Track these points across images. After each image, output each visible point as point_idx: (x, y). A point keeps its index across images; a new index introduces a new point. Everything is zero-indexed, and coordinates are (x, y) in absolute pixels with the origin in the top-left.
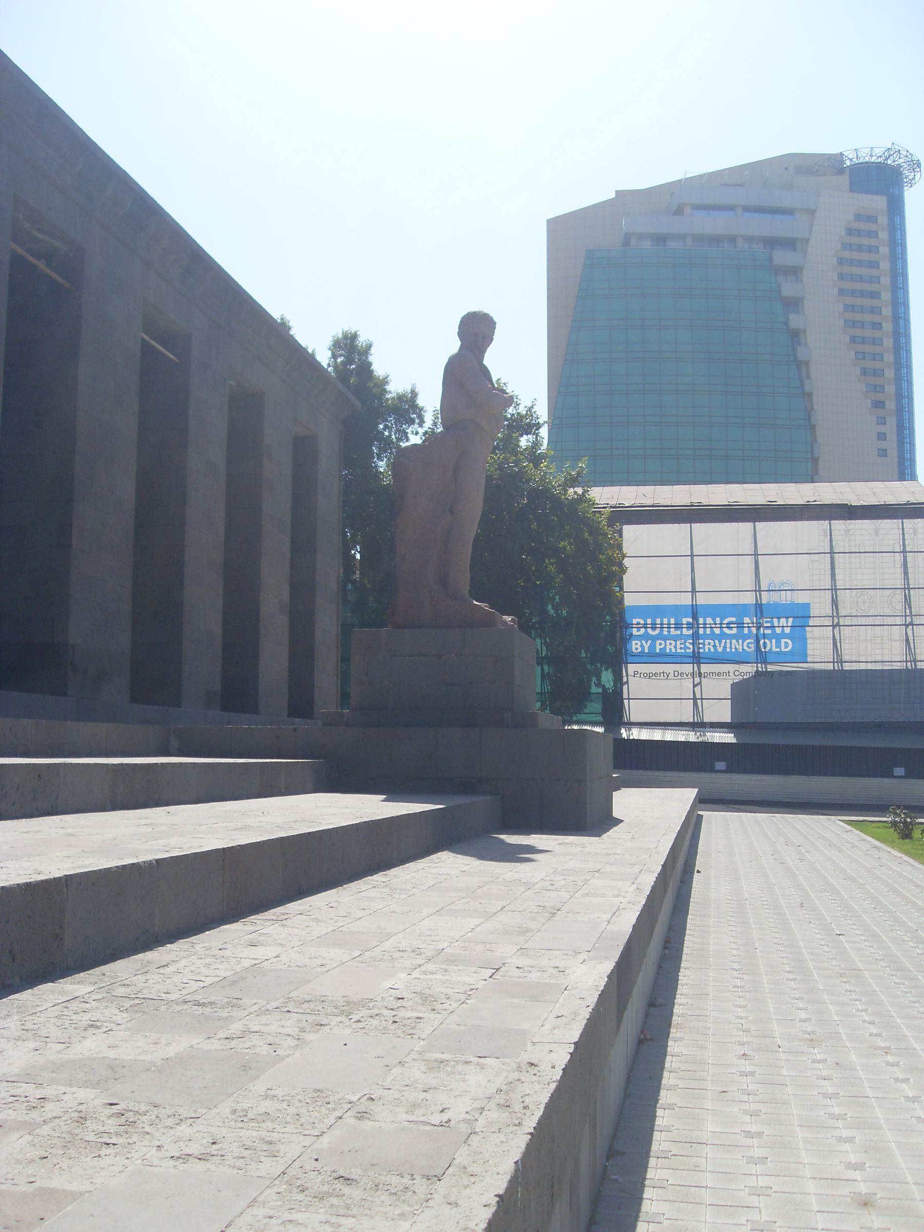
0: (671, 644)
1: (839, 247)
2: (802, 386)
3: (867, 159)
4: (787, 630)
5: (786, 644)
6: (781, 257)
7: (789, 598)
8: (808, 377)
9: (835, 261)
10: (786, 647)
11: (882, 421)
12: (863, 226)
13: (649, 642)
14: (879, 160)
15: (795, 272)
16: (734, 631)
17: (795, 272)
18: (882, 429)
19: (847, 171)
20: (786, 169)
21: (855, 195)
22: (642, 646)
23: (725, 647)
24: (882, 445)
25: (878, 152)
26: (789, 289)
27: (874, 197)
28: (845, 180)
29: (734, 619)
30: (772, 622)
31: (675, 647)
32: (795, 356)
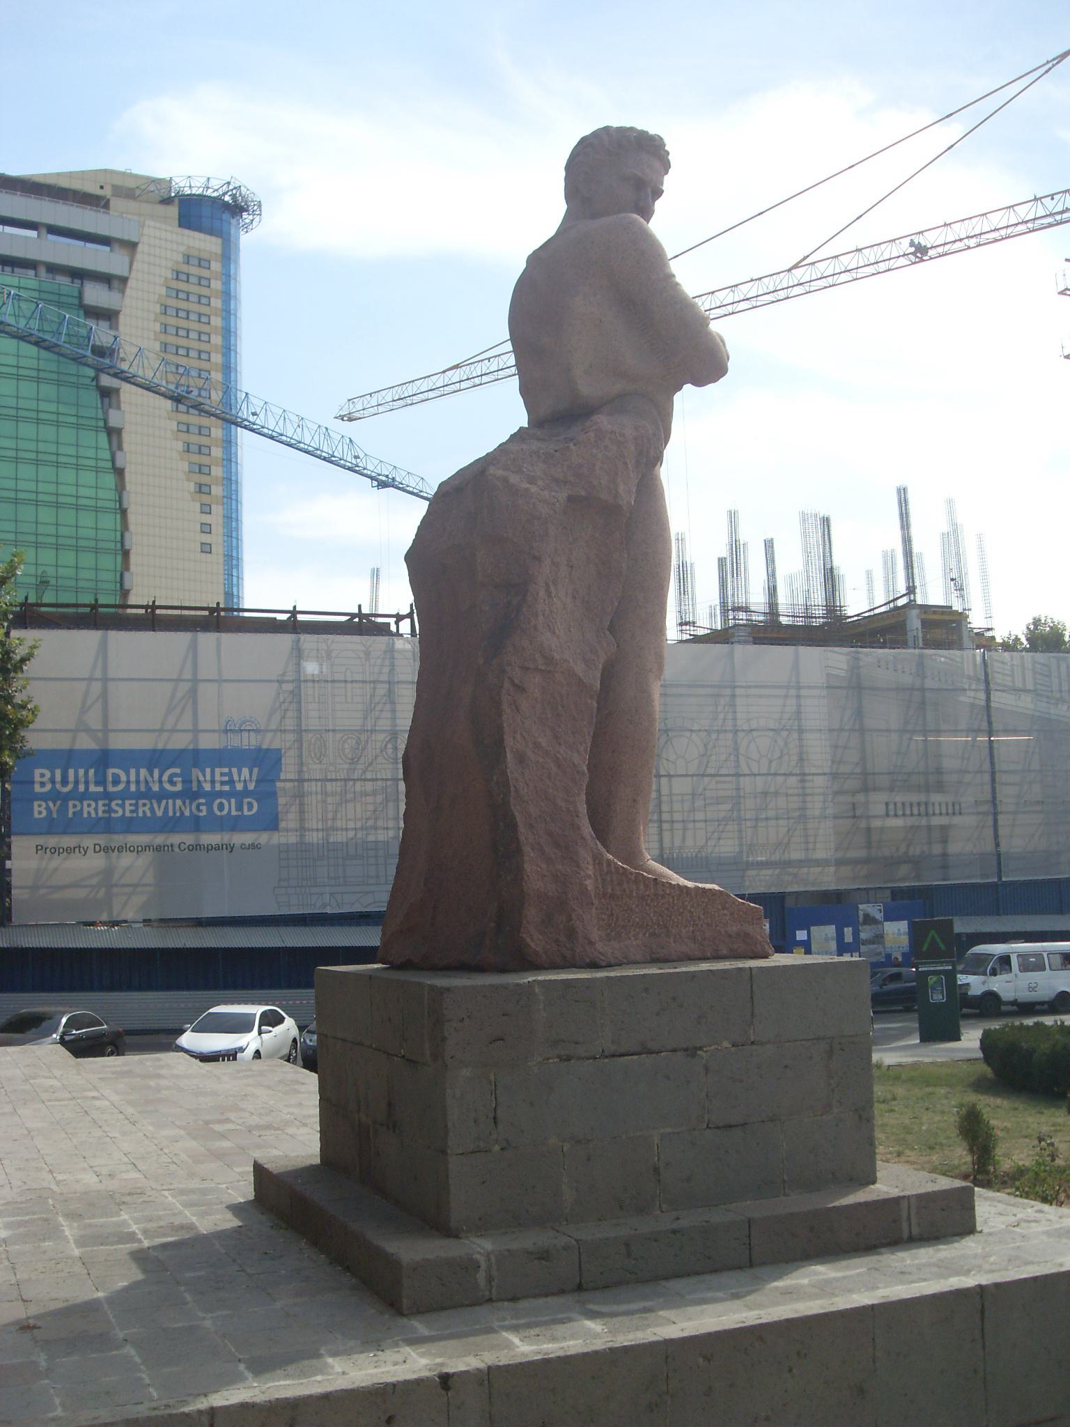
0: (89, 806)
1: (163, 291)
2: (113, 460)
3: (200, 192)
4: (251, 787)
5: (250, 804)
6: (95, 295)
7: (253, 742)
8: (120, 448)
9: (158, 309)
10: (250, 808)
11: (206, 509)
12: (194, 270)
13: (59, 803)
14: (215, 194)
15: (109, 316)
16: (179, 787)
17: (109, 316)
18: (206, 519)
19: (176, 202)
20: (102, 187)
21: (186, 232)
22: (48, 808)
23: (166, 808)
24: (206, 538)
25: (215, 184)
26: (102, 334)
27: (208, 237)
28: (173, 211)
29: (178, 771)
30: (230, 774)
31: (96, 809)
32: (106, 421)
